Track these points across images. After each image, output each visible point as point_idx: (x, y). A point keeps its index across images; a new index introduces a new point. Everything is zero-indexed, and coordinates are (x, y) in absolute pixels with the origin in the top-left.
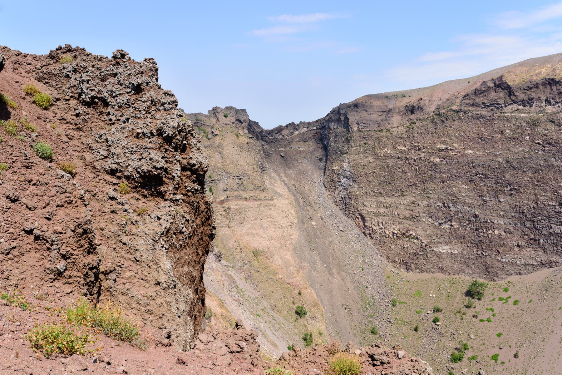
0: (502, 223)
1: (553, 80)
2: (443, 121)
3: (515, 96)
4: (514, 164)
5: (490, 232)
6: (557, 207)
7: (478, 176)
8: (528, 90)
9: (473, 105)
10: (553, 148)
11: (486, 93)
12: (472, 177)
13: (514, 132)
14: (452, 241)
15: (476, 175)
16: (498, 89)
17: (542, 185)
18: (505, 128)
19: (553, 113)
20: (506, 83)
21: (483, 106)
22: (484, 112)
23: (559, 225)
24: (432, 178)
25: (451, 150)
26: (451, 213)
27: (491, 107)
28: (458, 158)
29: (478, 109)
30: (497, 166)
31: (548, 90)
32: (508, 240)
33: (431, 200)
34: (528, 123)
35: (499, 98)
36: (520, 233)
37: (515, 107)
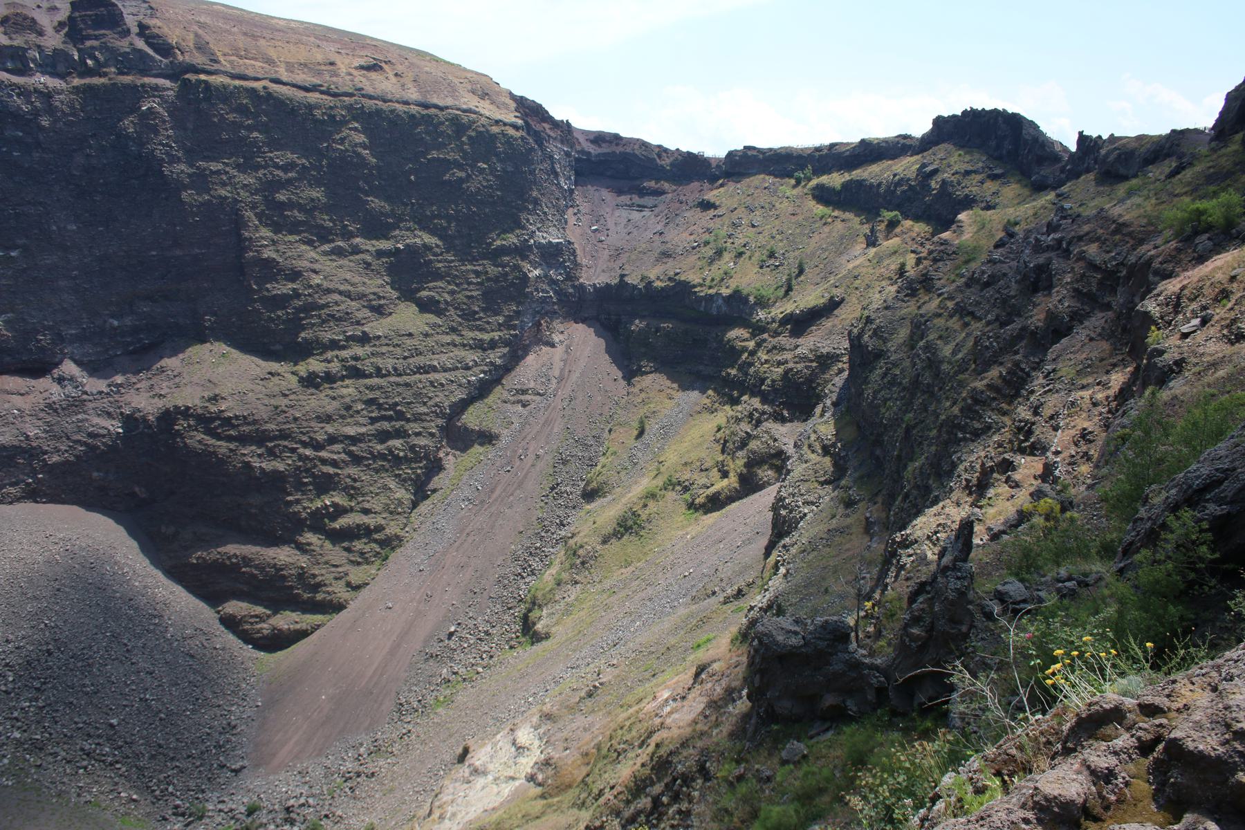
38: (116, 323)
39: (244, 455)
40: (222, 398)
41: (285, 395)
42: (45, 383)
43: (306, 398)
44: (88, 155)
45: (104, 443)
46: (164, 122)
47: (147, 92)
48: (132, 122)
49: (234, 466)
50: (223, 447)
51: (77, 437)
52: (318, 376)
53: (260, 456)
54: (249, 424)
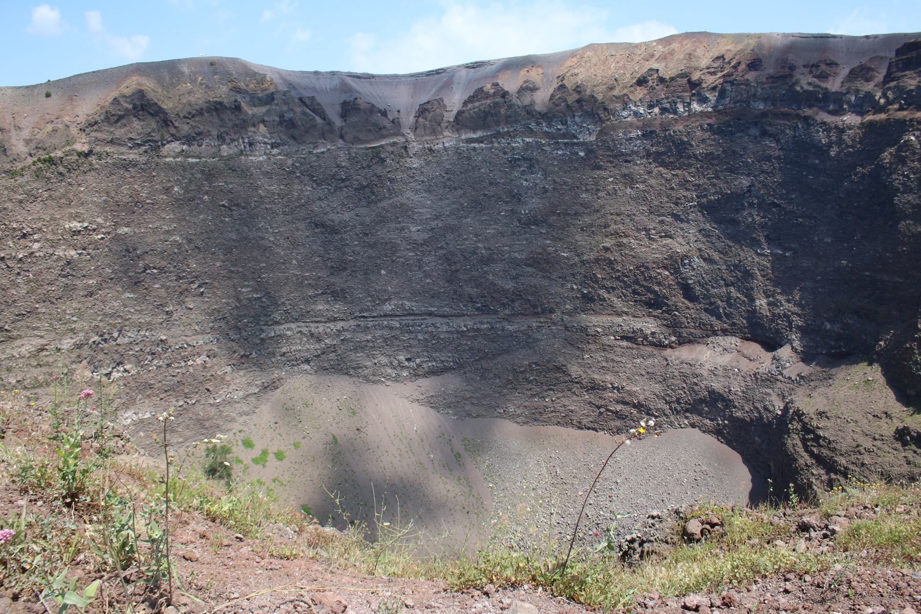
0: (201, 342)
1: (221, 103)
2: (61, 174)
3: (175, 127)
4: (199, 243)
5: (189, 363)
6: (264, 300)
7: (149, 271)
8: (190, 119)
9: (112, 142)
10: (242, 210)
11: (124, 121)
12: (139, 276)
13: (187, 190)
14: (135, 399)
15: (144, 272)
16: (140, 113)
17: (240, 269)
18: (172, 184)
19: (230, 158)
20: (156, 104)
21: (130, 145)
22: (132, 155)
23: (272, 325)
24: (69, 289)
25: (94, 230)
26: (120, 349)
27: (143, 148)
28: (107, 244)
29: (123, 149)
30: (176, 251)
31: (216, 120)
32: (216, 367)
33: (81, 334)
34: (202, 172)
35: (153, 131)
36: (225, 352)
37: (176, 146)
38: (828, 326)
39: (813, 474)
40: (827, 417)
41: (875, 439)
42: (767, 357)
43: (887, 449)
44: (853, 182)
45: (767, 417)
46: (914, 153)
47: (913, 126)
48: (891, 154)
49: (802, 479)
50: (804, 458)
51: (758, 405)
52: (909, 434)
53: (822, 481)
54: (829, 449)
